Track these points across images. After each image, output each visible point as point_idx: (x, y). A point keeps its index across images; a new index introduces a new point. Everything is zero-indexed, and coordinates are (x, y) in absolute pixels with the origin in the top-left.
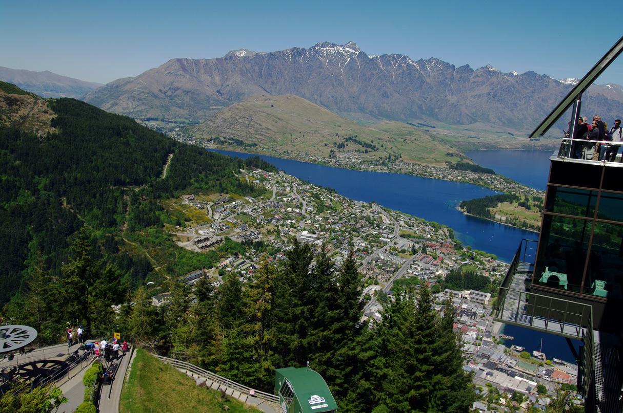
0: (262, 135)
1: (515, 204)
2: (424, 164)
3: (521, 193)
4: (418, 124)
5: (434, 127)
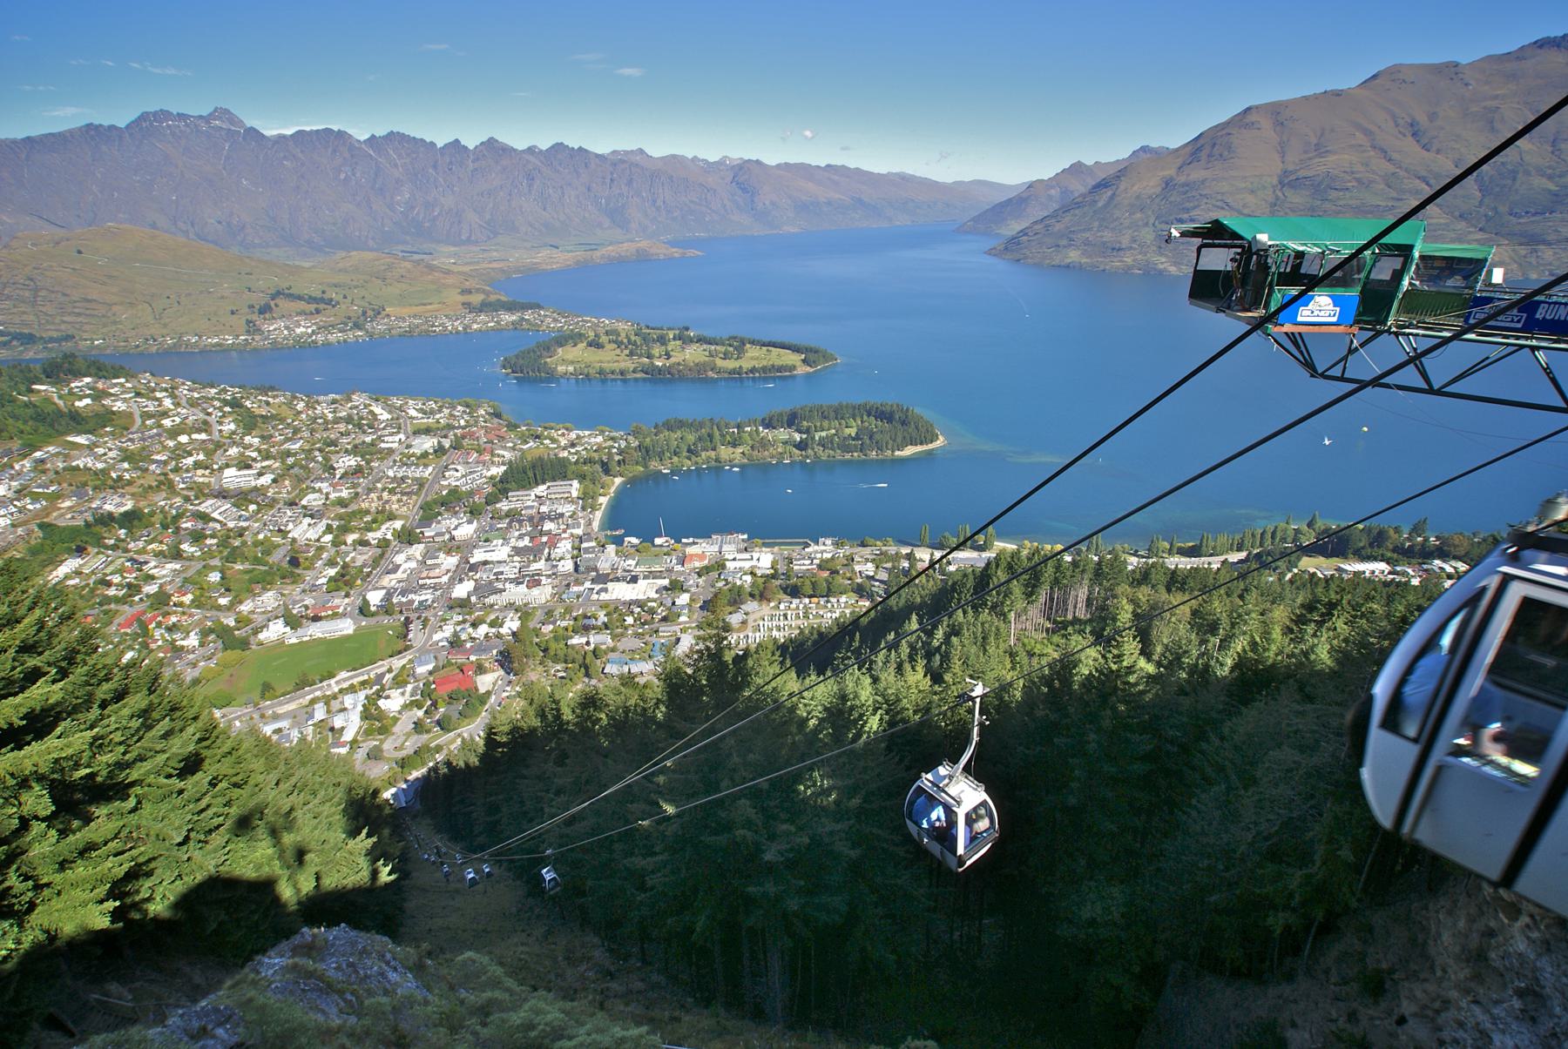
1: (582, 345)
5: (431, 254)
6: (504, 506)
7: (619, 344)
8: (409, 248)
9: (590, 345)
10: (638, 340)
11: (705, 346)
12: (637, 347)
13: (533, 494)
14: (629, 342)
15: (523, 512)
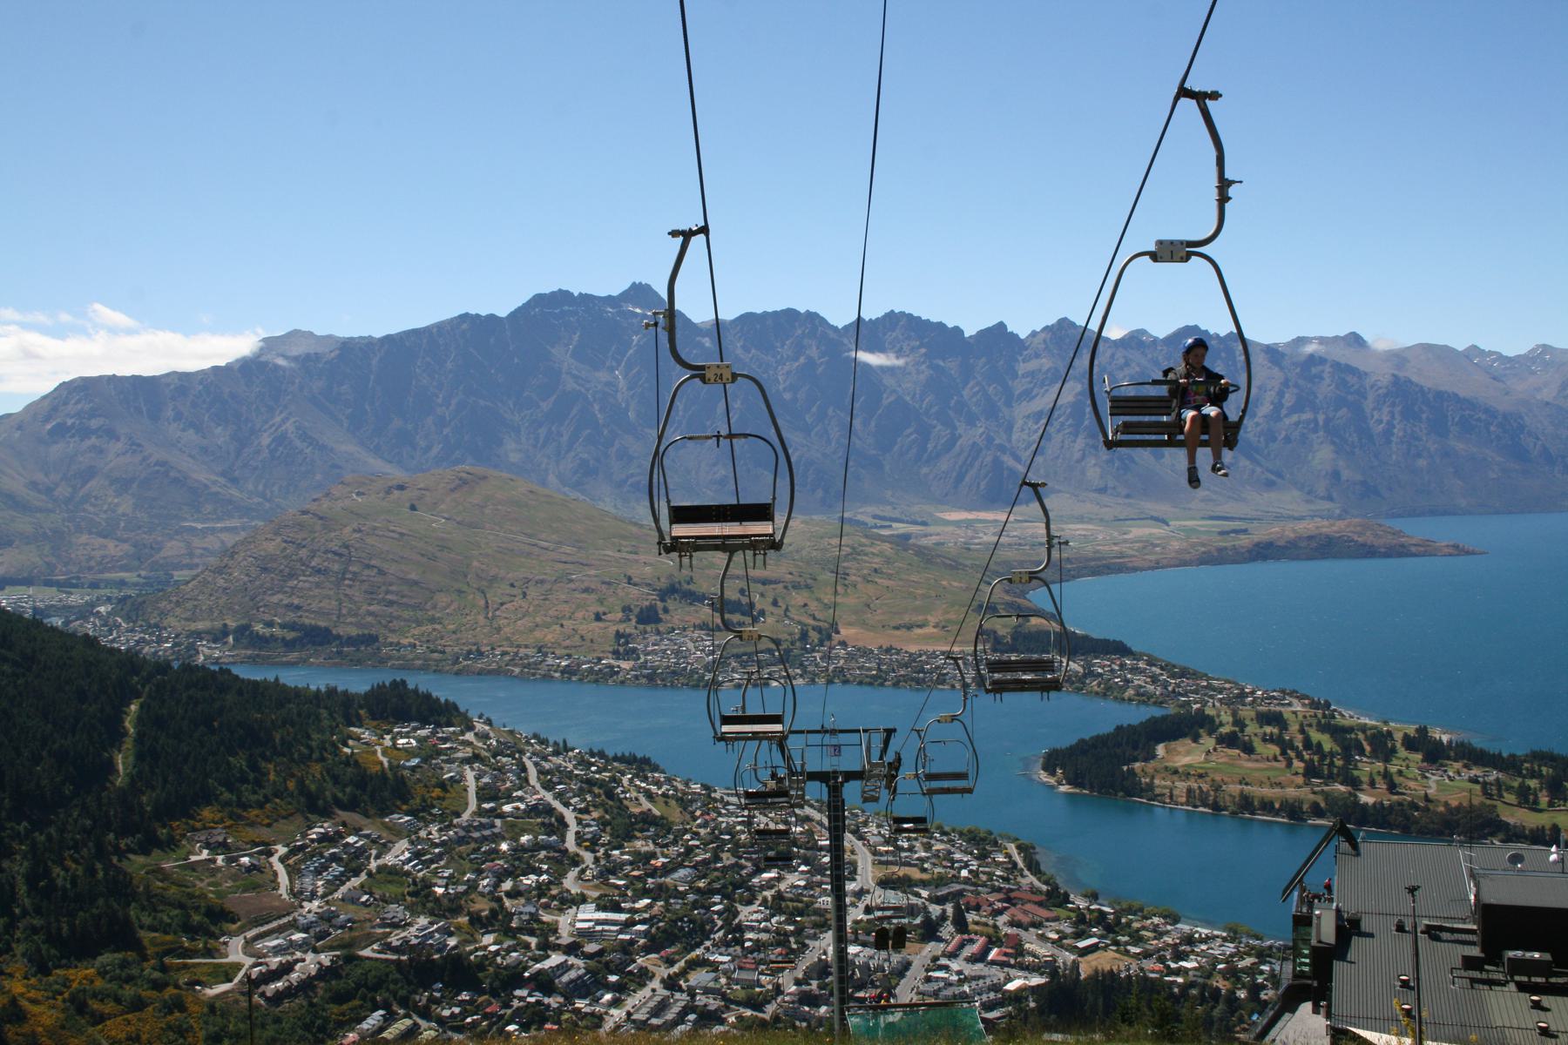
0: (391, 603)
1: (1209, 742)
2: (913, 649)
3: (1217, 704)
4: (875, 517)
7: (1285, 746)
8: (887, 511)
9: (1230, 741)
10: (1328, 744)
11: (1475, 772)
12: (1323, 756)
14: (1308, 743)
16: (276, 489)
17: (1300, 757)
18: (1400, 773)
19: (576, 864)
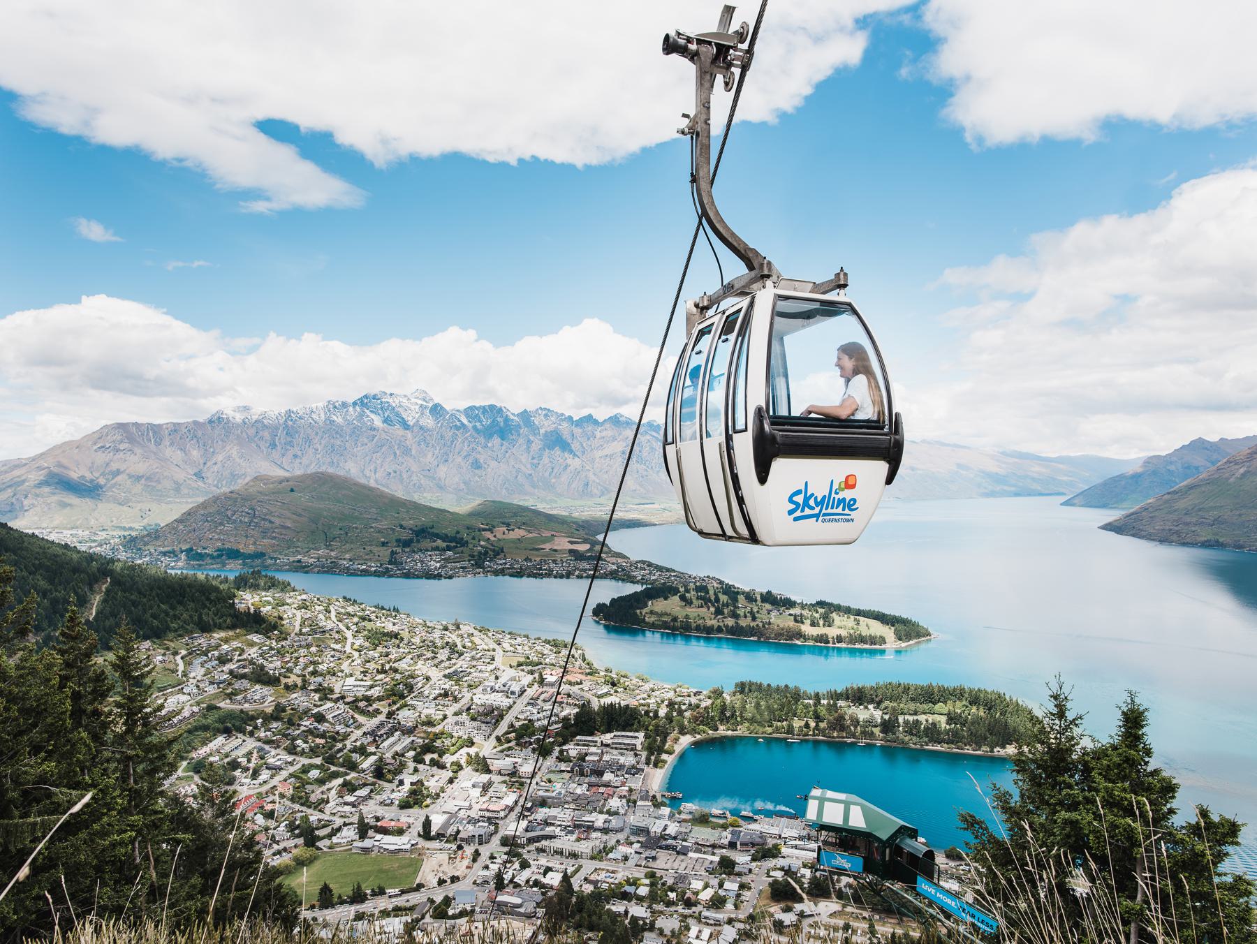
6: (572, 750)
13: (599, 741)
15: (587, 758)
16: (224, 483)
17: (713, 606)
18: (758, 612)
19: (349, 657)
